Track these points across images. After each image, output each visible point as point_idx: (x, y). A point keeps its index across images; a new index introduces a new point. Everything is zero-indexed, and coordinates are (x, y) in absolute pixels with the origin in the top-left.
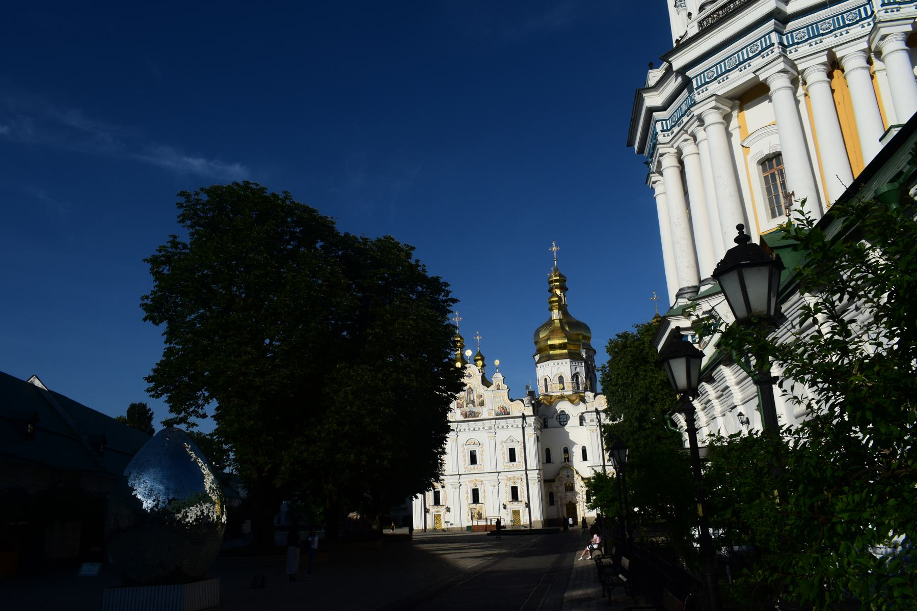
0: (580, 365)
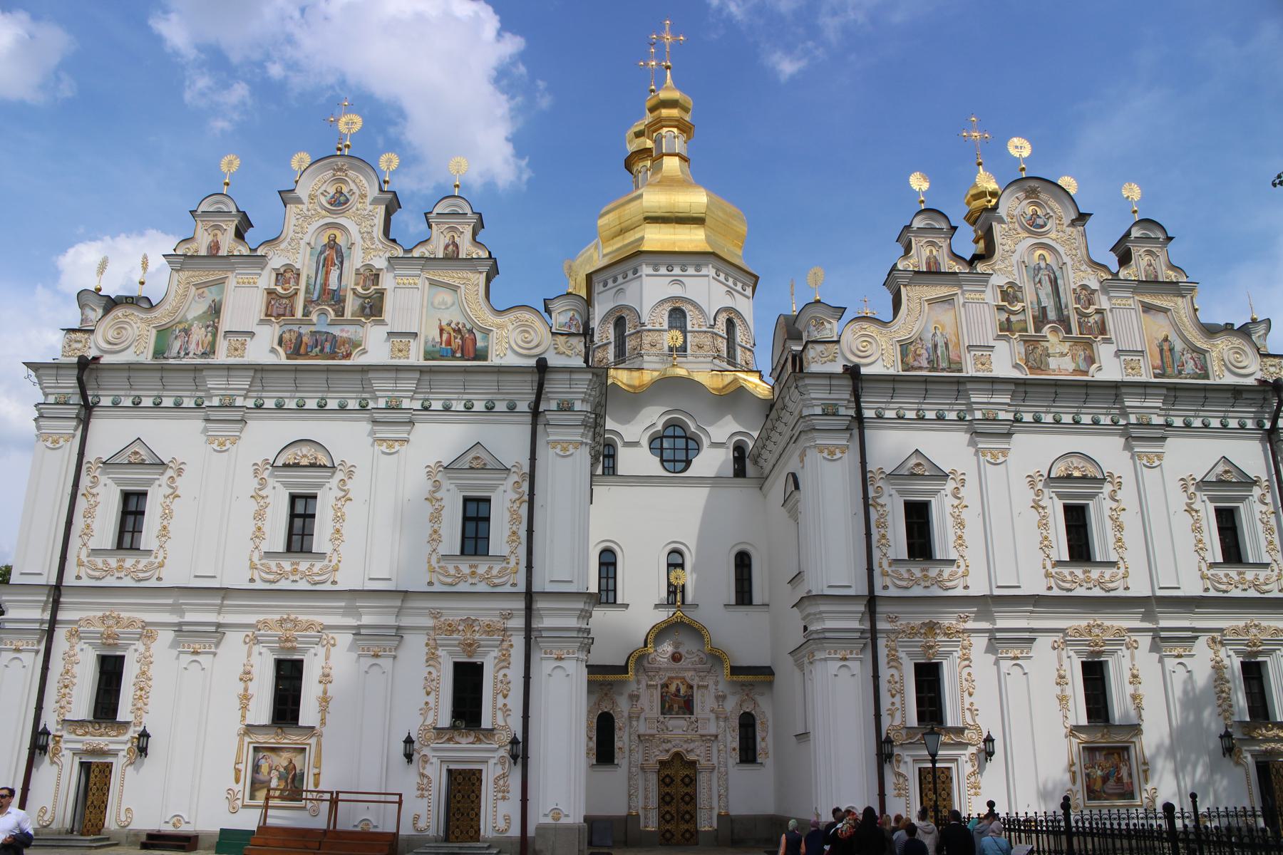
0: (739, 287)
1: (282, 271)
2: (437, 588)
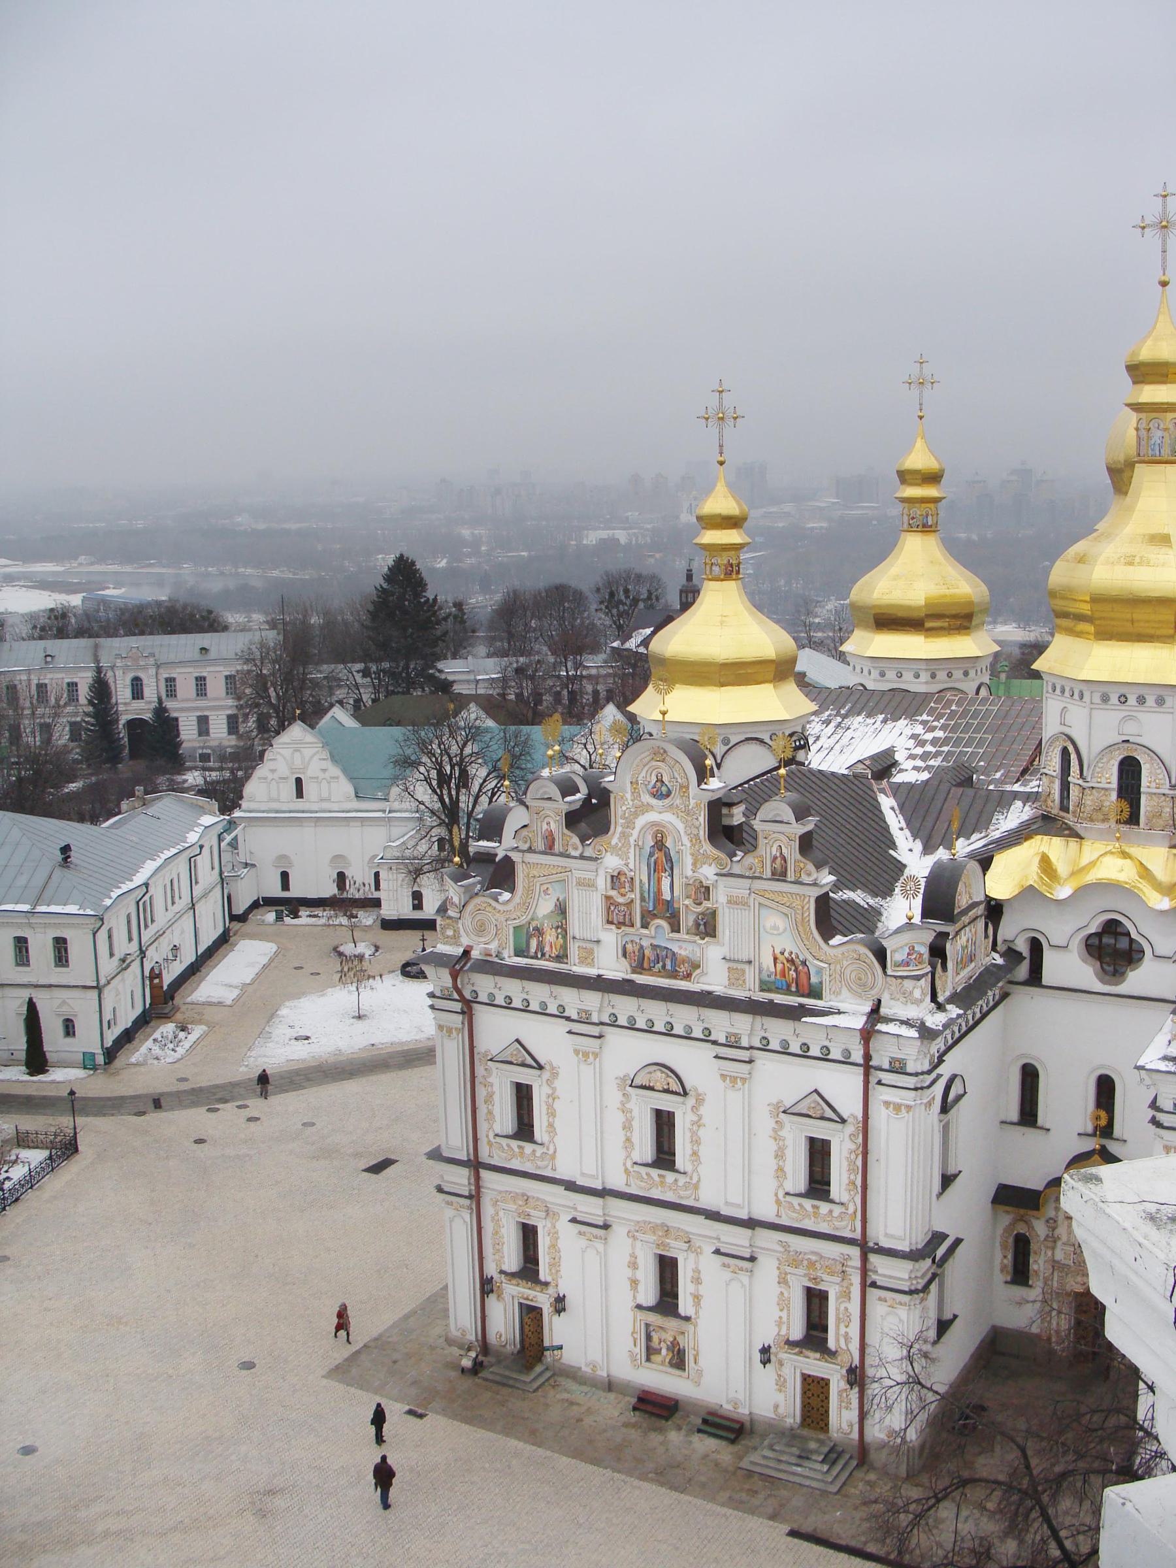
1: (616, 874)
2: (785, 1221)
